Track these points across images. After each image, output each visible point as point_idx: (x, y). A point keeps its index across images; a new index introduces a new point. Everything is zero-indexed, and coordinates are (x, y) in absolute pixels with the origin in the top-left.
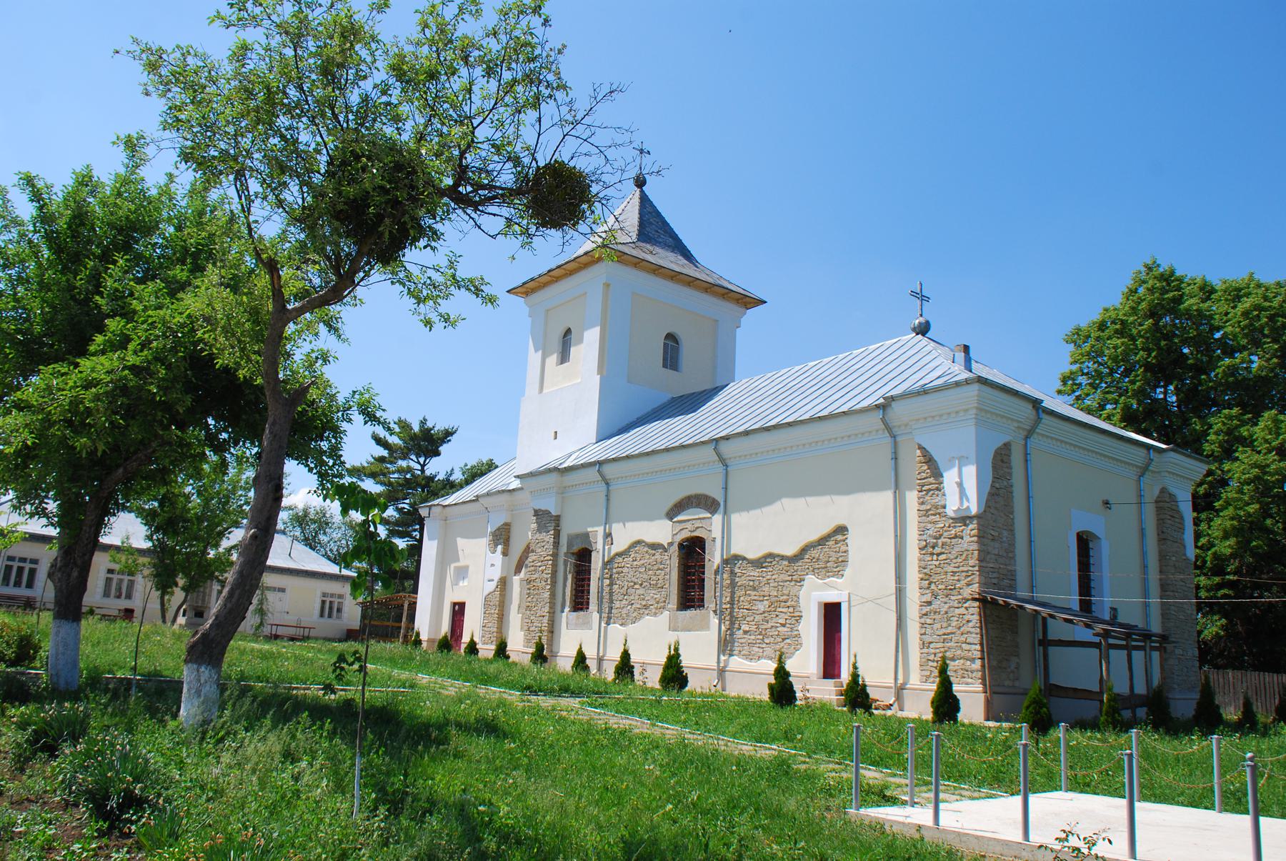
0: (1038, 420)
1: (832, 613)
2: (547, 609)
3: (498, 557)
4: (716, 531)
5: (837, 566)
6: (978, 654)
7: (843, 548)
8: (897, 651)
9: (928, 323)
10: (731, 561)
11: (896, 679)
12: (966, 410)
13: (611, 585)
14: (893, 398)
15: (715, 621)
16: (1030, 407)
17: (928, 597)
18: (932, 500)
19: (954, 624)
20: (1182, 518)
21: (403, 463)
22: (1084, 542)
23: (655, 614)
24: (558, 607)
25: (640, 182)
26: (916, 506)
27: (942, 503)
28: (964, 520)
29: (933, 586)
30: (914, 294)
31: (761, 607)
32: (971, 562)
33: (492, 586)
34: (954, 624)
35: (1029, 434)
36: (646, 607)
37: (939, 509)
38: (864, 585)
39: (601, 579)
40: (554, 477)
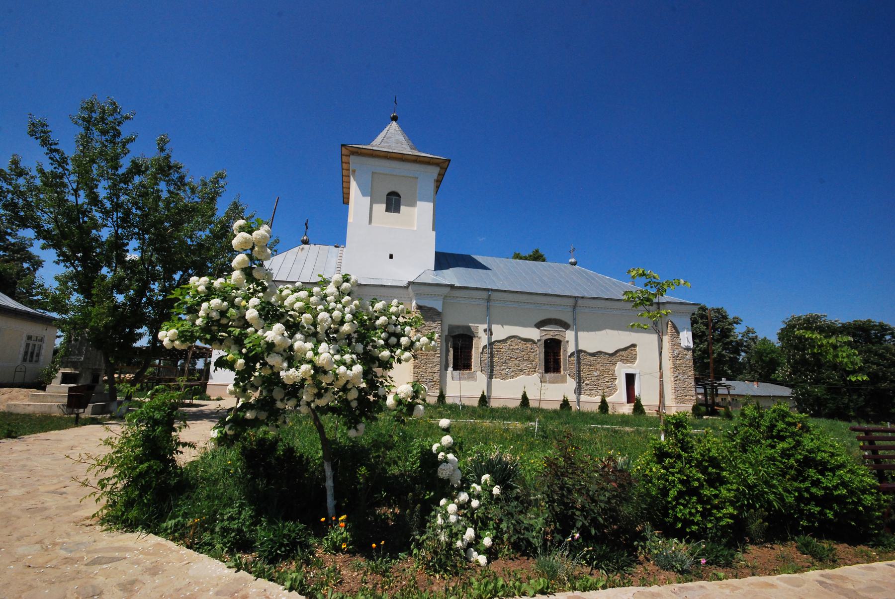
1: (630, 379)
5: (634, 358)
28: (688, 349)
31: (595, 374)
36: (521, 370)
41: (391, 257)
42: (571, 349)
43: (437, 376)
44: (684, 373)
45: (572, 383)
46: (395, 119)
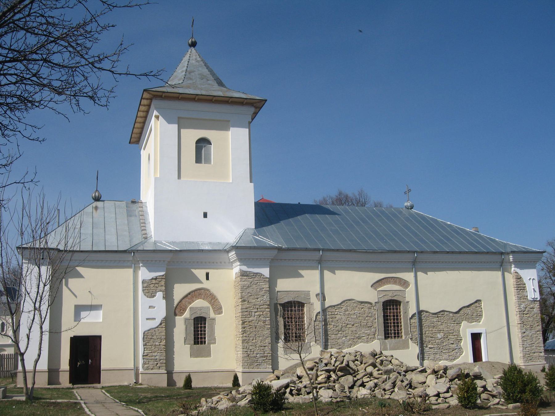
1: (476, 338)
10: (420, 312)
17: (524, 330)
28: (534, 301)
29: (525, 326)
31: (439, 336)
36: (359, 338)
41: (205, 215)
42: (413, 310)
43: (268, 350)
45: (414, 349)
46: (193, 45)
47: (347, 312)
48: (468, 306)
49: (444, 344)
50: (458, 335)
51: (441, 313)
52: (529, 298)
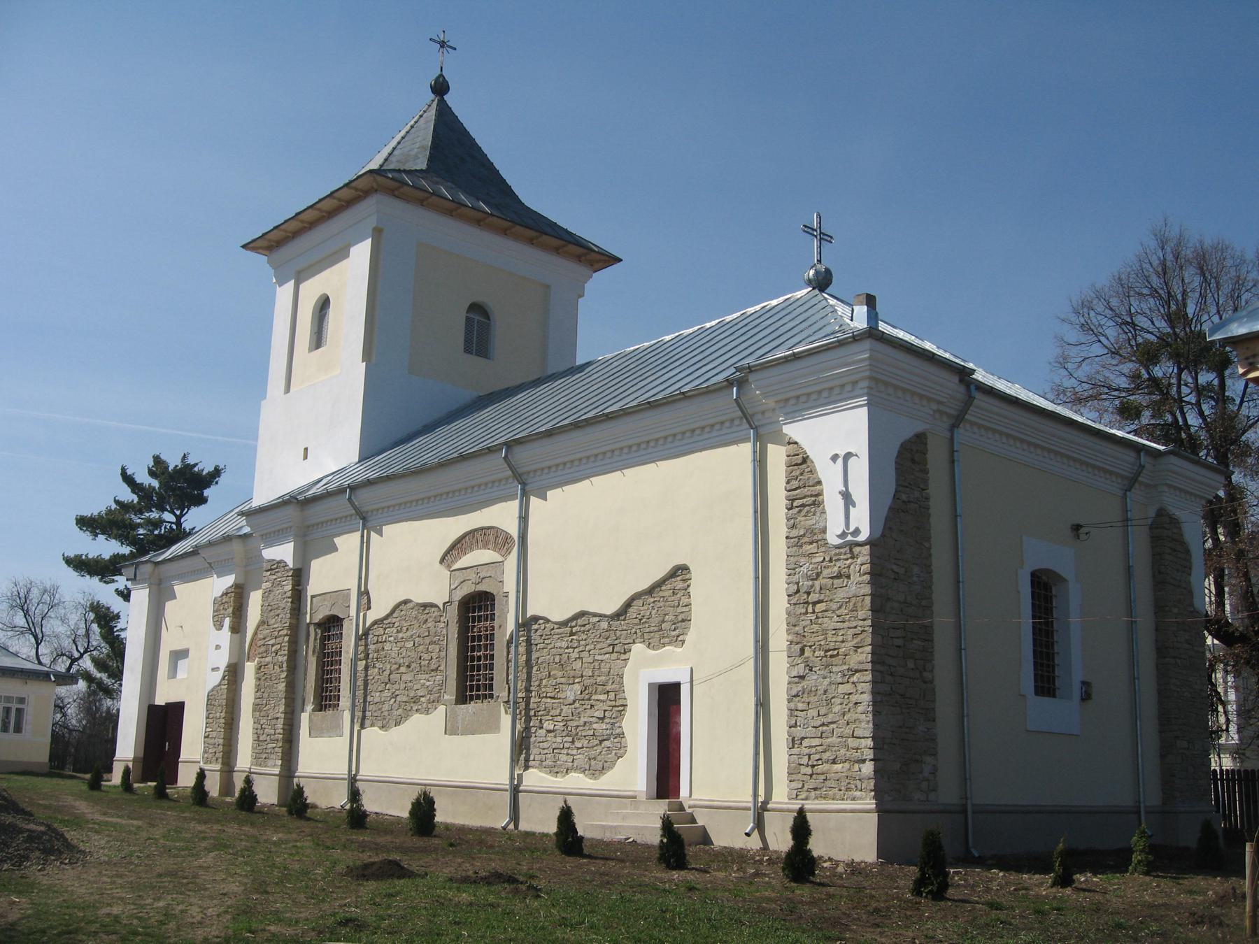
0: (970, 399)
1: (667, 699)
2: (282, 708)
3: (225, 636)
4: (510, 585)
6: (869, 754)
7: (684, 600)
8: (757, 754)
9: (828, 271)
10: (527, 624)
11: (755, 795)
12: (855, 383)
13: (366, 668)
14: (750, 369)
15: (506, 720)
16: (956, 379)
17: (800, 669)
18: (805, 522)
19: (836, 709)
20: (1188, 552)
21: (154, 515)
22: (1044, 587)
23: (427, 712)
24: (299, 707)
25: (440, 88)
26: (783, 531)
27: (822, 524)
29: (808, 652)
30: (808, 229)
31: (572, 692)
32: (861, 614)
33: (216, 678)
34: (836, 709)
35: (957, 421)
36: (416, 700)
37: (816, 535)
38: (713, 657)
39: (355, 660)
40: (291, 511)
44: (831, 654)
47: (400, 635)
48: (650, 591)
49: (583, 719)
50: (619, 692)
51: (580, 622)
52: (832, 538)
